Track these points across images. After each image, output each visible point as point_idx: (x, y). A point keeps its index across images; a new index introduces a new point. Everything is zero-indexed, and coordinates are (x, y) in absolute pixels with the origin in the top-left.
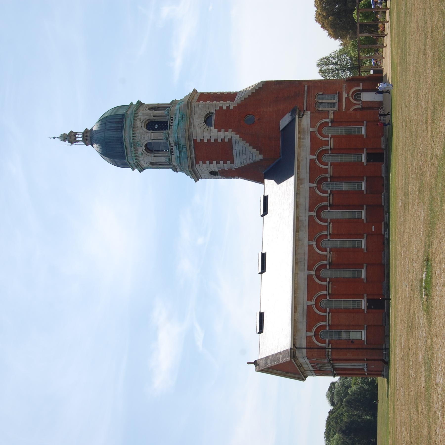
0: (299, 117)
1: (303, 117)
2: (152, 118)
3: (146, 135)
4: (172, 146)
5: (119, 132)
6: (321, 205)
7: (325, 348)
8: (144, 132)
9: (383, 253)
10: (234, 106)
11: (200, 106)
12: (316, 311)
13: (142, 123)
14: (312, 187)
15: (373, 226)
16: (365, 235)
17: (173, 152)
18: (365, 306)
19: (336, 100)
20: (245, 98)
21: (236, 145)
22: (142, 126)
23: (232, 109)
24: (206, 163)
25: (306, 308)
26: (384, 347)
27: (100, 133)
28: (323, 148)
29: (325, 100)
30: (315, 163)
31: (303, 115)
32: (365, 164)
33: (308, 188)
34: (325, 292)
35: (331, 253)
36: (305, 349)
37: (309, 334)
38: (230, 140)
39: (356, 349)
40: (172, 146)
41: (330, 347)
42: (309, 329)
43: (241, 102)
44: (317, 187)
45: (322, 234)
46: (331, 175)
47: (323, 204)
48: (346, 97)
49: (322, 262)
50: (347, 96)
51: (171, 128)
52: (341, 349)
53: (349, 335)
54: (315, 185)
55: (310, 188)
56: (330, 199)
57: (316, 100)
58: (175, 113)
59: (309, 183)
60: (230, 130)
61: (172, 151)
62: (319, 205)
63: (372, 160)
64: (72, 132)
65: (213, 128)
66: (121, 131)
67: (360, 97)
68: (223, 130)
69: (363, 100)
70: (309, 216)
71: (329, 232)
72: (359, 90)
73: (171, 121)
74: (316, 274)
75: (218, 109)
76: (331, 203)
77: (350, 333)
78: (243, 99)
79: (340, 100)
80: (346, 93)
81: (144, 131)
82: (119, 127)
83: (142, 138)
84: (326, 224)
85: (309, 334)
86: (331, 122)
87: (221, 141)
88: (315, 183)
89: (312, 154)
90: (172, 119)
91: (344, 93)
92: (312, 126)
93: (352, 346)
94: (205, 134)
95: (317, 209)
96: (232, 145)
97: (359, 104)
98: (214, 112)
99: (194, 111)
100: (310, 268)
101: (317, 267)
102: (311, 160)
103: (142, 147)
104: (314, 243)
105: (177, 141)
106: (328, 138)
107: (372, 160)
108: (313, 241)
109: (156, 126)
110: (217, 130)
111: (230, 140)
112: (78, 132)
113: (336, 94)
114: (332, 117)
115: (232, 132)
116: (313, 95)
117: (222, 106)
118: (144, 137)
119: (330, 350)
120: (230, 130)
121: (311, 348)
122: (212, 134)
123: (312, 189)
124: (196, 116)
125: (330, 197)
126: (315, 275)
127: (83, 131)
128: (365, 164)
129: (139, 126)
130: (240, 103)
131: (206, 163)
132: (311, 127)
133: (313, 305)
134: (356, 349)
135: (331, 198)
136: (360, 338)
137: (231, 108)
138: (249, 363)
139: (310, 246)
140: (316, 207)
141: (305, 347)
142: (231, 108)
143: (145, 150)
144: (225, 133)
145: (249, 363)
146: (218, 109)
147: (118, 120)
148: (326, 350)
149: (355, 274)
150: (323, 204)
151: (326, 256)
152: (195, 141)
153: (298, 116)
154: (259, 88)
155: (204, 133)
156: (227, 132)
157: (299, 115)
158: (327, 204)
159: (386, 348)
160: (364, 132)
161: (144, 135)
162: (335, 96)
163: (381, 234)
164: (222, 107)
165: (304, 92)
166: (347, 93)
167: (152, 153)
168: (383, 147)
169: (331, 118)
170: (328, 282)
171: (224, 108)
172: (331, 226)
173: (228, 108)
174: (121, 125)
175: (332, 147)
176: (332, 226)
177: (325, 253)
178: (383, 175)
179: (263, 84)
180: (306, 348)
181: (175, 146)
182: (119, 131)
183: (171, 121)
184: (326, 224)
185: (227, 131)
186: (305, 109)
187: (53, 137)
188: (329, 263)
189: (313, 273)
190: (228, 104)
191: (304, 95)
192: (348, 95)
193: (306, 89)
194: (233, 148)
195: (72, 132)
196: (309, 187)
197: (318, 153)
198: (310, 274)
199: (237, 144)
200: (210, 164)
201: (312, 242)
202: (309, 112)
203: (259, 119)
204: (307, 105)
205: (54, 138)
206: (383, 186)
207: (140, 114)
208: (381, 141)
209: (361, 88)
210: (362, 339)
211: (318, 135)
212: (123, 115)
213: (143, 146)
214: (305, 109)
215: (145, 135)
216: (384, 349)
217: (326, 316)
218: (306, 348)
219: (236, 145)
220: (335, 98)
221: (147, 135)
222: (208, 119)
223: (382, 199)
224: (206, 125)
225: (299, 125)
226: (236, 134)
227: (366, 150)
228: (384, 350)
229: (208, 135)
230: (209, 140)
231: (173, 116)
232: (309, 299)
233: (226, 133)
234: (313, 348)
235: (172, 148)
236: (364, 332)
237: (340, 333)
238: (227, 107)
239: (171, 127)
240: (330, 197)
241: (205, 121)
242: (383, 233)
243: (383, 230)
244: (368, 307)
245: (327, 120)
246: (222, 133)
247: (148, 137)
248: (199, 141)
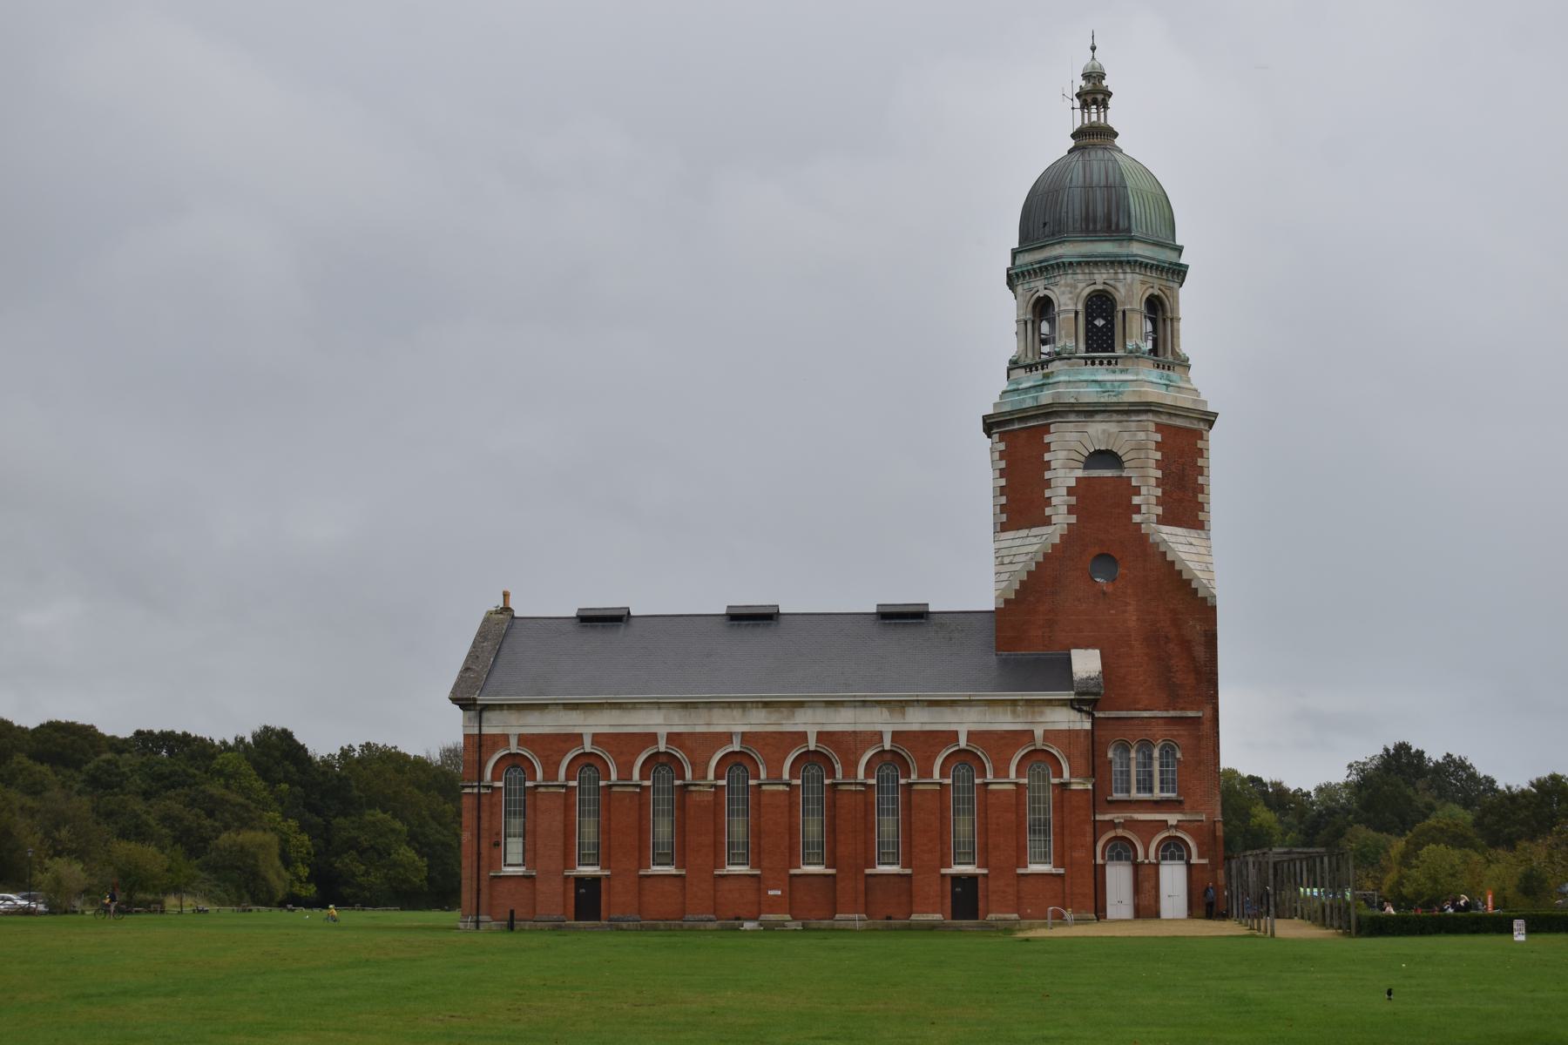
0: (1071, 700)
1: (1076, 712)
2: (1120, 308)
3: (1070, 299)
4: (1043, 369)
5: (1078, 225)
6: (835, 763)
7: (480, 778)
8: (1078, 290)
9: (712, 916)
10: (1143, 526)
11: (1142, 435)
12: (570, 757)
13: (1105, 283)
14: (882, 738)
15: (779, 893)
16: (759, 872)
17: (1031, 371)
18: (582, 873)
19: (1157, 794)
20: (1165, 552)
21: (1035, 536)
22: (1095, 283)
23: (1133, 521)
24: (1001, 459)
25: (577, 730)
26: (482, 918)
27: (1081, 173)
28: (987, 765)
29: (1161, 766)
30: (946, 745)
31: (1080, 710)
32: (944, 871)
33: (878, 728)
34: (614, 776)
35: (713, 790)
36: (477, 732)
37: (513, 742)
38: (1047, 521)
39: (479, 854)
40: (1043, 369)
41: (482, 791)
42: (524, 740)
43: (1155, 543)
44: (884, 751)
45: (761, 767)
46: (916, 787)
47: (838, 767)
48: (1166, 821)
49: (690, 767)
50: (1170, 823)
51: (1086, 364)
52: (479, 818)
53: (515, 836)
54: (887, 746)
55: (880, 734)
56: (851, 784)
57: (1160, 741)
58: (1127, 370)
59: (893, 732)
61: (1034, 369)
62: (835, 758)
63: (958, 890)
64: (1110, 94)
65: (1080, 473)
66: (1081, 231)
67: (1172, 858)
69: (1161, 867)
70: (806, 733)
71: (765, 784)
72: (1190, 857)
73: (1105, 362)
74: (658, 753)
75: (1133, 484)
76: (840, 787)
77: (520, 836)
78: (1162, 549)
79: (1158, 805)
80: (1179, 821)
81: (1082, 290)
82: (1095, 223)
83: (1063, 289)
84: (786, 776)
85: (513, 742)
86: (1063, 784)
87: (1048, 498)
88: (892, 746)
89: (970, 734)
90: (1113, 362)
91: (1179, 817)
92: (1048, 734)
93: (485, 844)
94: (1062, 455)
95: (825, 752)
96: (1038, 526)
97: (1147, 856)
98: (1124, 475)
99: (1127, 421)
100: (672, 738)
101: (678, 755)
102: (956, 733)
103: (1045, 289)
104: (736, 747)
105: (1051, 381)
106: (1017, 777)
107: (958, 890)
108: (741, 743)
109: (1100, 322)
110: (1074, 484)
111: (1047, 521)
112: (1108, 111)
113: (1179, 795)
114: (1074, 787)
115: (1068, 524)
116: (1175, 733)
117: (1142, 493)
118: (1063, 293)
119: (476, 790)
120: (1073, 519)
121: (480, 746)
122: (1061, 473)
123: (877, 737)
124: (1112, 428)
125: (856, 784)
126: (656, 750)
127: (1110, 123)
128: (944, 871)
129: (1096, 276)
130: (1151, 540)
131: (1001, 459)
132: (1045, 731)
133: (583, 748)
134: (479, 854)
135: (853, 788)
136: (508, 862)
137: (1136, 518)
138: (506, 595)
139: (728, 737)
140: (830, 751)
141: (483, 733)
142: (1136, 518)
143: (1039, 297)
144: (1066, 507)
145: (506, 595)
146: (1133, 484)
147: (1114, 219)
148: (475, 781)
149: (663, 849)
150: (836, 766)
151: (705, 778)
152: (1045, 429)
153: (1073, 697)
154: (1196, 590)
155: (1065, 453)
156: (1066, 512)
157: (1079, 701)
158: (837, 776)
159: (481, 924)
160: (1034, 868)
161: (1071, 293)
162: (1174, 792)
163: (760, 914)
164: (1139, 495)
165: (1182, 709)
166: (1180, 824)
167: (1034, 316)
168: (992, 916)
169: (1070, 783)
170: (639, 783)
171: (1136, 500)
172: (781, 788)
173: (1137, 509)
174: (1098, 227)
175: (992, 787)
176: (779, 792)
177: (711, 775)
178: (914, 917)
179: (1204, 599)
180: (480, 735)
181: (1041, 377)
182: (1084, 226)
183: (1105, 362)
184: (786, 776)
186: (1098, 714)
187: (1096, 44)
188: (686, 786)
189: (662, 747)
190: (1149, 509)
191: (1174, 709)
192: (1172, 826)
193: (1191, 714)
194: (1033, 529)
195: (1110, 94)
196: (881, 732)
197: (975, 751)
198: (659, 739)
199: (1038, 538)
200: (1000, 469)
201: (740, 740)
202: (1088, 726)
203: (1104, 593)
204: (1146, 718)
205: (1093, 49)
206: (889, 918)
207: (1129, 276)
208: (1008, 913)
209: (1195, 860)
210: (505, 865)
211: (1026, 751)
212: (1129, 230)
213: (1047, 292)
214: (1098, 714)
215: (1070, 296)
216: (478, 918)
217: (557, 780)
218: (480, 735)
219: (1035, 536)
220: (1168, 791)
221: (1069, 302)
223: (851, 916)
224: (1087, 454)
225: (1049, 702)
226: (1062, 536)
227: (983, 874)
228: (475, 918)
229: (1060, 462)
230: (1047, 466)
231: (1119, 366)
232: (597, 738)
233: (1064, 509)
234: (480, 751)
235: (1040, 368)
236: (520, 870)
237: (520, 814)
238: (1139, 507)
239: (1089, 362)
240: (856, 784)
241: (1098, 452)
242: (763, 917)
243: (771, 915)
244: (580, 880)
245: (1066, 775)
246: (1066, 498)
247: (1066, 305)
248: (1047, 439)
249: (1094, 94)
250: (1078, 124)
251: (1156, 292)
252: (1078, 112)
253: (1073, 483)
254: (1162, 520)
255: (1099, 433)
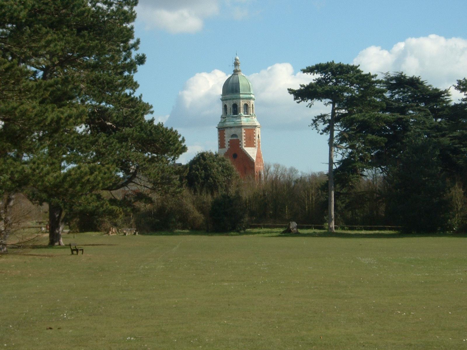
2: (238, 107)
38: (225, 147)
60: (229, 147)
65: (230, 138)
68: (229, 144)
94: (227, 135)
98: (238, 138)
111: (225, 147)
120: (229, 147)
152: (224, 130)
185: (229, 145)
222: (234, 135)
241: (233, 135)
249: (236, 64)
250: (234, 69)
251: (246, 103)
252: (234, 67)
253: (229, 140)
254: (245, 147)
255: (233, 131)
